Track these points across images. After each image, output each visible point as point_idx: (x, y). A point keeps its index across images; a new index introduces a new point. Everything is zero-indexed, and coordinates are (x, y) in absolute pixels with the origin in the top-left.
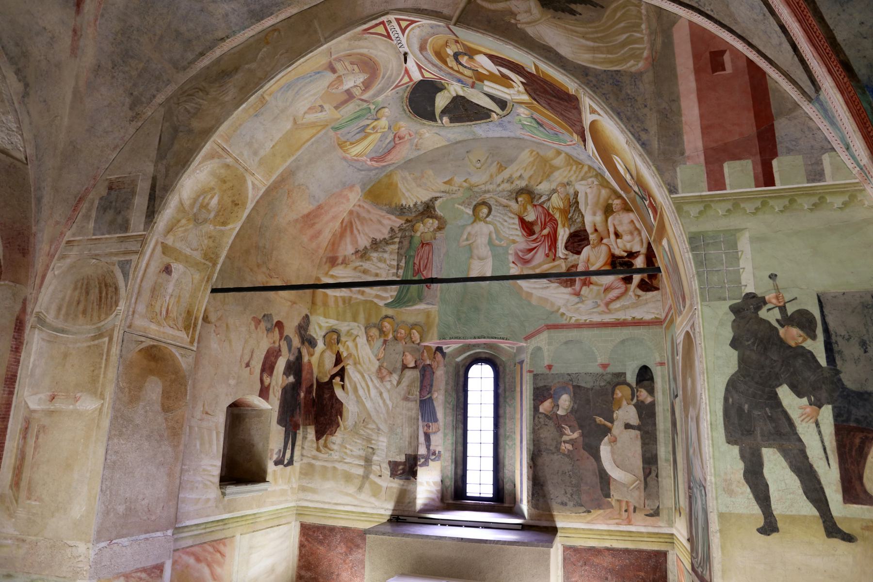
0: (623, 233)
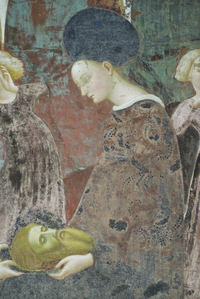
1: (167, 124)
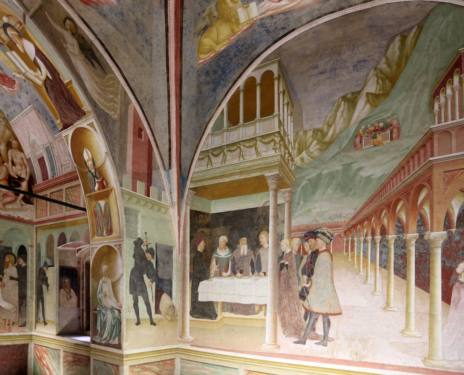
0: (17, 164)
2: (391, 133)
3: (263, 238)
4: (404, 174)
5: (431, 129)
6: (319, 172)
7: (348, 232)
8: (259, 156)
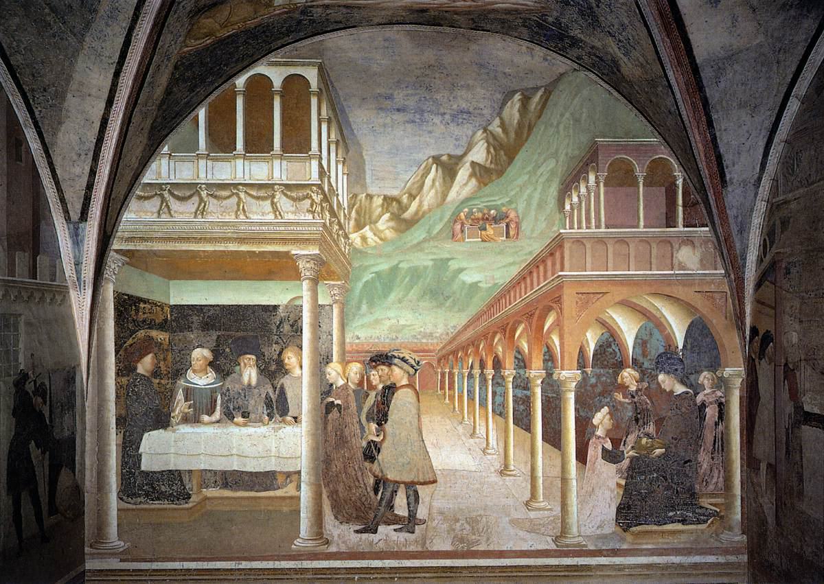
1: (695, 401)
2: (507, 226)
3: (290, 358)
4: (526, 288)
5: (561, 233)
6: (396, 262)
7: (443, 359)
8: (280, 218)
